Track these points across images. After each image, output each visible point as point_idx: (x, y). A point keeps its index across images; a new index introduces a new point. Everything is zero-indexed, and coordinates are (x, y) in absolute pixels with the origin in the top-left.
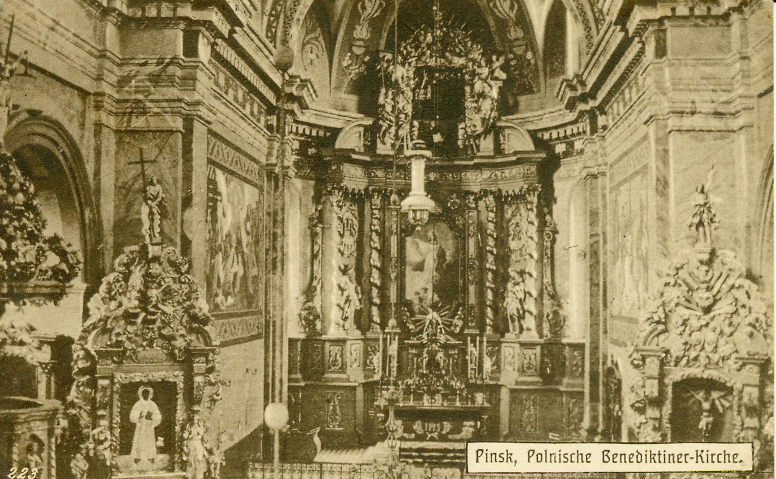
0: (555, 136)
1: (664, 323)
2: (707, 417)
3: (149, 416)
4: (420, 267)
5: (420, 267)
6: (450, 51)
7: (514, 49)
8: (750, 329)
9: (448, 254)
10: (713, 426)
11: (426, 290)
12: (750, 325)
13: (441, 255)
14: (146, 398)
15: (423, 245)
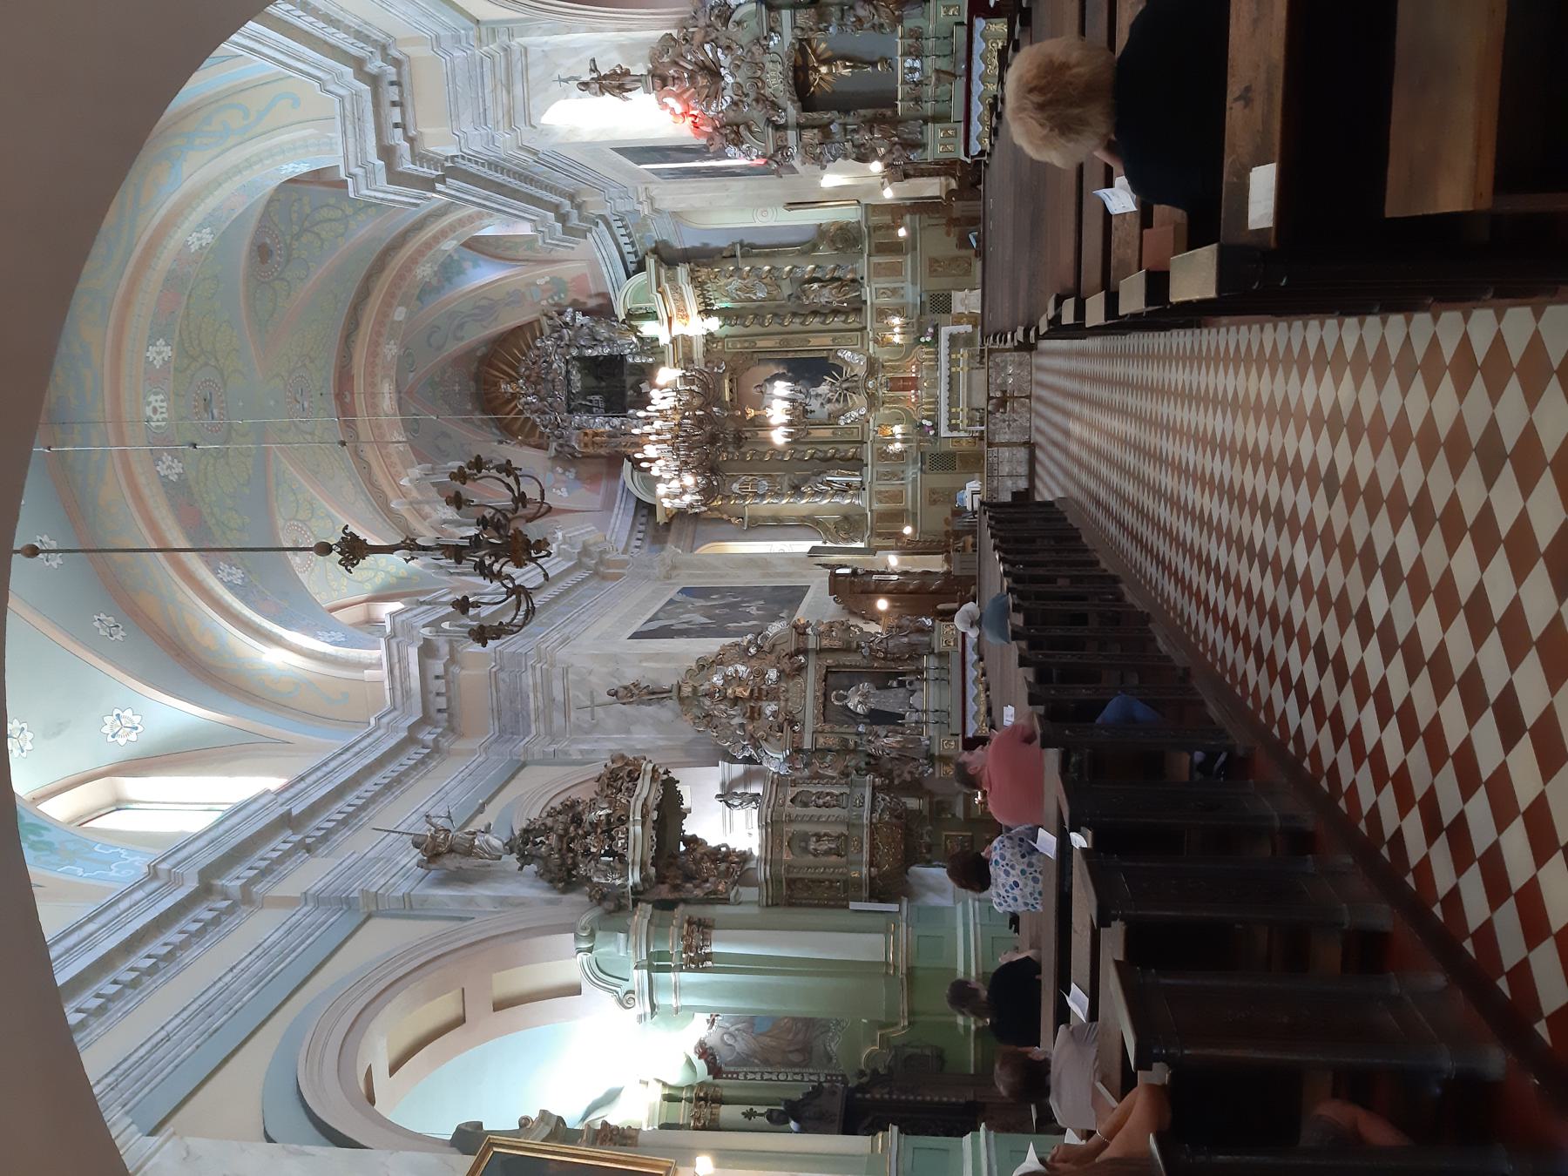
0: (628, 248)
1: (738, 127)
2: (836, 66)
3: (866, 696)
6: (547, 373)
7: (536, 300)
8: (730, 25)
10: (847, 60)
11: (818, 395)
12: (726, 24)
14: (846, 697)
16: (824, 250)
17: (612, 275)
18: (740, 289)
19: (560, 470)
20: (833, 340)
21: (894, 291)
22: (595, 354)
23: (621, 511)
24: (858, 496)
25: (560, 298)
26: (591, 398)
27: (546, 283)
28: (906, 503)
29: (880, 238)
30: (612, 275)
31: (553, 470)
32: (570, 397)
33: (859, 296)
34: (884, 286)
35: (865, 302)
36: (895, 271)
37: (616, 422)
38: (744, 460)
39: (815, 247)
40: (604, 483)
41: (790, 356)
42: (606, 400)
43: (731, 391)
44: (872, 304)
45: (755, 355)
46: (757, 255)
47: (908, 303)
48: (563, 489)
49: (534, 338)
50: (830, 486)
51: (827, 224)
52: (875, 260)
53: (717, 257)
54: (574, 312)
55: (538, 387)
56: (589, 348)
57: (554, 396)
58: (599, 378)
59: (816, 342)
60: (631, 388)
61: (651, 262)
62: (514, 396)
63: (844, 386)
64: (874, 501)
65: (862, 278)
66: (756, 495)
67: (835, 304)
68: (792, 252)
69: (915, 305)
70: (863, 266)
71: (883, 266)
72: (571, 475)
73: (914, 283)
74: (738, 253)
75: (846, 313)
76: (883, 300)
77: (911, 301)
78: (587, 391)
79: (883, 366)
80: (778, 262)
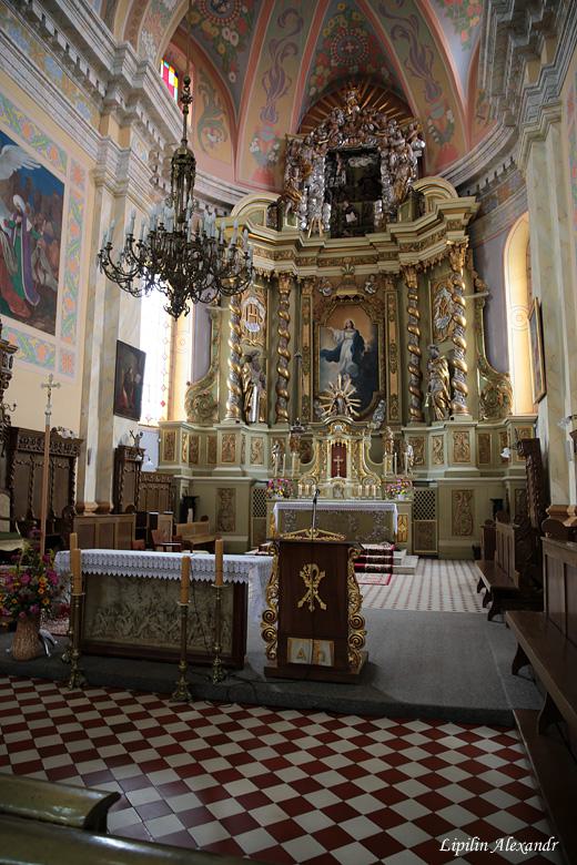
4: (335, 356)
5: (335, 356)
7: (432, 114)
9: (366, 341)
13: (358, 341)
15: (337, 333)
16: (481, 381)
17: (455, 172)
18: (444, 301)
19: (277, 147)
20: (394, 395)
21: (440, 455)
22: (383, 172)
23: (228, 190)
24: (233, 416)
25: (435, 137)
26: (344, 174)
27: (449, 121)
28: (223, 466)
29: (495, 439)
30: (455, 172)
31: (276, 140)
32: (347, 154)
33: (436, 420)
34: (445, 444)
35: (430, 425)
36: (460, 456)
37: (321, 194)
38: (280, 310)
39: (485, 372)
40: (264, 186)
41: (381, 356)
42: (341, 188)
43: (347, 297)
44: (428, 432)
45: (381, 321)
46: (476, 314)
47: (427, 469)
48: (257, 149)
49: (398, 119)
50: (248, 390)
51: (508, 384)
52: (472, 433)
53: (475, 274)
54: (422, 149)
55: (352, 125)
56: (388, 165)
57: (344, 138)
58: (361, 182)
59: (394, 378)
60: (350, 206)
61: (470, 202)
62: (343, 105)
63: (339, 400)
64: (224, 432)
65: (452, 419)
66: (238, 317)
67: (427, 395)
68: (481, 351)
69: (425, 475)
70: (465, 417)
71: (465, 441)
72: (271, 157)
73: (447, 474)
74: (478, 295)
75: (420, 407)
76: (431, 443)
77: (430, 472)
78: (350, 172)
79: (358, 441)
80: (470, 333)
